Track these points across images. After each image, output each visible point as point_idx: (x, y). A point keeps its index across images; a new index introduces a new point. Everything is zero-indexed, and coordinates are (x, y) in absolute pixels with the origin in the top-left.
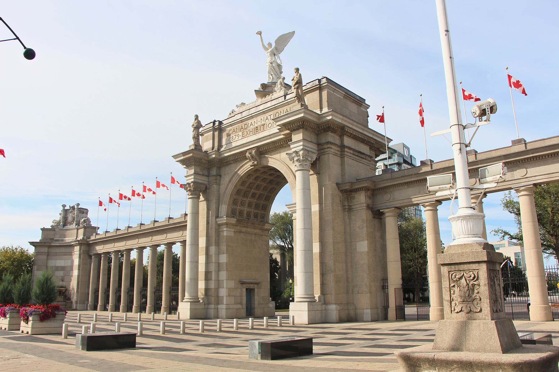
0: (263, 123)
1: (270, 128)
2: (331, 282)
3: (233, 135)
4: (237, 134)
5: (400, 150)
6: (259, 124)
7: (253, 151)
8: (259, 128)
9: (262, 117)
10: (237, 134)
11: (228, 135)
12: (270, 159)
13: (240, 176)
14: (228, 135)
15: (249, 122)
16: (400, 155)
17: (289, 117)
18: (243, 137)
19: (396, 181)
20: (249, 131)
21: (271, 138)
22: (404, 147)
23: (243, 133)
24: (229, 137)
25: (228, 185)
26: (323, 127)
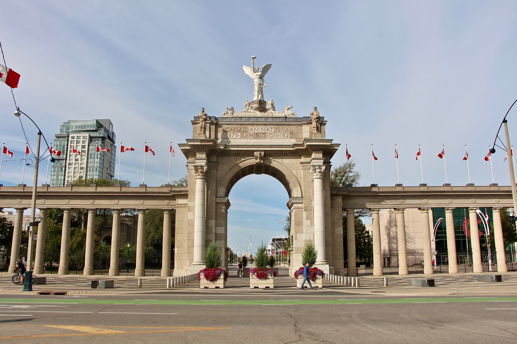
0: (263, 132)
3: (231, 133)
4: (235, 133)
5: (106, 125)
7: (262, 153)
9: (263, 127)
11: (225, 132)
12: (272, 161)
13: (241, 168)
14: (225, 132)
15: (250, 127)
16: (107, 131)
17: (318, 142)
18: (242, 137)
19: (360, 194)
20: (249, 134)
21: (281, 148)
22: (110, 123)
24: (226, 133)
25: (228, 172)
26: (327, 152)
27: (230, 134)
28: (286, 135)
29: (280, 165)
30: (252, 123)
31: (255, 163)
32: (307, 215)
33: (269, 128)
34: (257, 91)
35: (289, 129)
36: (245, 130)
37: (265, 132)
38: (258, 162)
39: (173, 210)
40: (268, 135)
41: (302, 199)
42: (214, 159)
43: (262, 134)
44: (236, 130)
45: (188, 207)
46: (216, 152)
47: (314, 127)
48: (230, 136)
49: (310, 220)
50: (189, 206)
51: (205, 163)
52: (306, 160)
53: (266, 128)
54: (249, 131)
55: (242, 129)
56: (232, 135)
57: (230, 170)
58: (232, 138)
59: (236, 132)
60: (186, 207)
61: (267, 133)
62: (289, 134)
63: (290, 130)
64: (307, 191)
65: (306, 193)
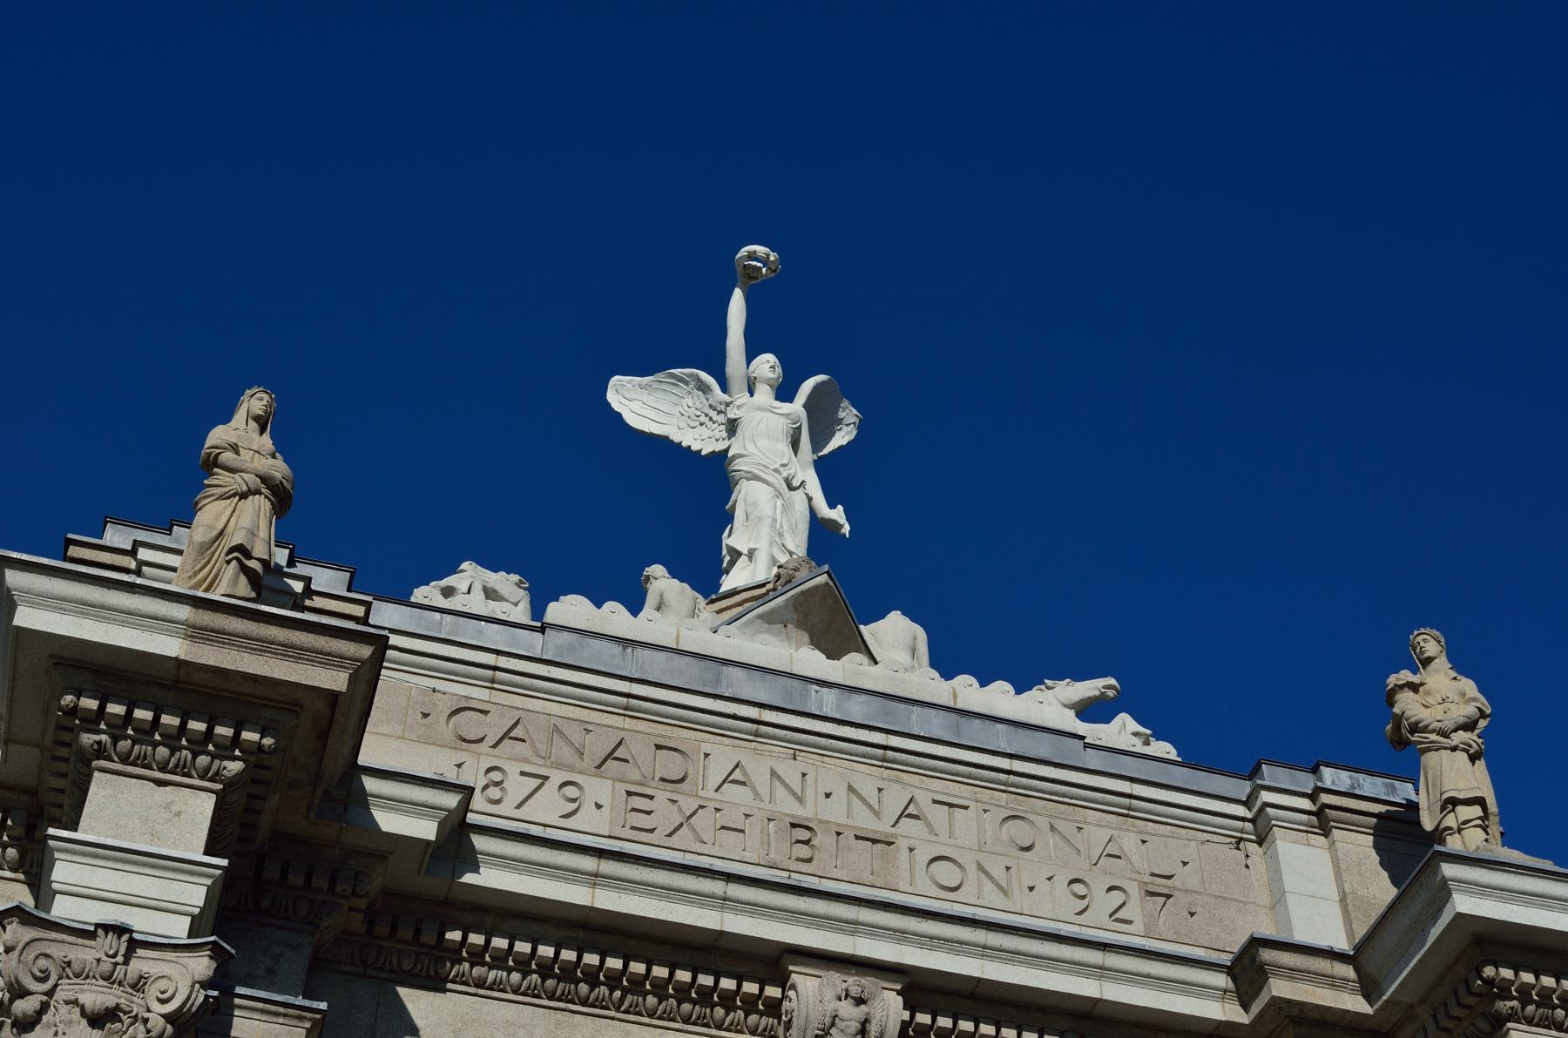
0: (866, 822)
1: (952, 896)
4: (557, 777)
6: (835, 811)
8: (823, 839)
9: (867, 778)
10: (557, 777)
15: (722, 755)
21: (1102, 972)
27: (495, 776)
33: (924, 799)
34: (768, 522)
36: (670, 765)
37: (882, 827)
43: (849, 835)
46: (320, 882)
51: (178, 928)
53: (894, 802)
55: (639, 749)
56: (517, 787)
59: (559, 766)
61: (902, 844)
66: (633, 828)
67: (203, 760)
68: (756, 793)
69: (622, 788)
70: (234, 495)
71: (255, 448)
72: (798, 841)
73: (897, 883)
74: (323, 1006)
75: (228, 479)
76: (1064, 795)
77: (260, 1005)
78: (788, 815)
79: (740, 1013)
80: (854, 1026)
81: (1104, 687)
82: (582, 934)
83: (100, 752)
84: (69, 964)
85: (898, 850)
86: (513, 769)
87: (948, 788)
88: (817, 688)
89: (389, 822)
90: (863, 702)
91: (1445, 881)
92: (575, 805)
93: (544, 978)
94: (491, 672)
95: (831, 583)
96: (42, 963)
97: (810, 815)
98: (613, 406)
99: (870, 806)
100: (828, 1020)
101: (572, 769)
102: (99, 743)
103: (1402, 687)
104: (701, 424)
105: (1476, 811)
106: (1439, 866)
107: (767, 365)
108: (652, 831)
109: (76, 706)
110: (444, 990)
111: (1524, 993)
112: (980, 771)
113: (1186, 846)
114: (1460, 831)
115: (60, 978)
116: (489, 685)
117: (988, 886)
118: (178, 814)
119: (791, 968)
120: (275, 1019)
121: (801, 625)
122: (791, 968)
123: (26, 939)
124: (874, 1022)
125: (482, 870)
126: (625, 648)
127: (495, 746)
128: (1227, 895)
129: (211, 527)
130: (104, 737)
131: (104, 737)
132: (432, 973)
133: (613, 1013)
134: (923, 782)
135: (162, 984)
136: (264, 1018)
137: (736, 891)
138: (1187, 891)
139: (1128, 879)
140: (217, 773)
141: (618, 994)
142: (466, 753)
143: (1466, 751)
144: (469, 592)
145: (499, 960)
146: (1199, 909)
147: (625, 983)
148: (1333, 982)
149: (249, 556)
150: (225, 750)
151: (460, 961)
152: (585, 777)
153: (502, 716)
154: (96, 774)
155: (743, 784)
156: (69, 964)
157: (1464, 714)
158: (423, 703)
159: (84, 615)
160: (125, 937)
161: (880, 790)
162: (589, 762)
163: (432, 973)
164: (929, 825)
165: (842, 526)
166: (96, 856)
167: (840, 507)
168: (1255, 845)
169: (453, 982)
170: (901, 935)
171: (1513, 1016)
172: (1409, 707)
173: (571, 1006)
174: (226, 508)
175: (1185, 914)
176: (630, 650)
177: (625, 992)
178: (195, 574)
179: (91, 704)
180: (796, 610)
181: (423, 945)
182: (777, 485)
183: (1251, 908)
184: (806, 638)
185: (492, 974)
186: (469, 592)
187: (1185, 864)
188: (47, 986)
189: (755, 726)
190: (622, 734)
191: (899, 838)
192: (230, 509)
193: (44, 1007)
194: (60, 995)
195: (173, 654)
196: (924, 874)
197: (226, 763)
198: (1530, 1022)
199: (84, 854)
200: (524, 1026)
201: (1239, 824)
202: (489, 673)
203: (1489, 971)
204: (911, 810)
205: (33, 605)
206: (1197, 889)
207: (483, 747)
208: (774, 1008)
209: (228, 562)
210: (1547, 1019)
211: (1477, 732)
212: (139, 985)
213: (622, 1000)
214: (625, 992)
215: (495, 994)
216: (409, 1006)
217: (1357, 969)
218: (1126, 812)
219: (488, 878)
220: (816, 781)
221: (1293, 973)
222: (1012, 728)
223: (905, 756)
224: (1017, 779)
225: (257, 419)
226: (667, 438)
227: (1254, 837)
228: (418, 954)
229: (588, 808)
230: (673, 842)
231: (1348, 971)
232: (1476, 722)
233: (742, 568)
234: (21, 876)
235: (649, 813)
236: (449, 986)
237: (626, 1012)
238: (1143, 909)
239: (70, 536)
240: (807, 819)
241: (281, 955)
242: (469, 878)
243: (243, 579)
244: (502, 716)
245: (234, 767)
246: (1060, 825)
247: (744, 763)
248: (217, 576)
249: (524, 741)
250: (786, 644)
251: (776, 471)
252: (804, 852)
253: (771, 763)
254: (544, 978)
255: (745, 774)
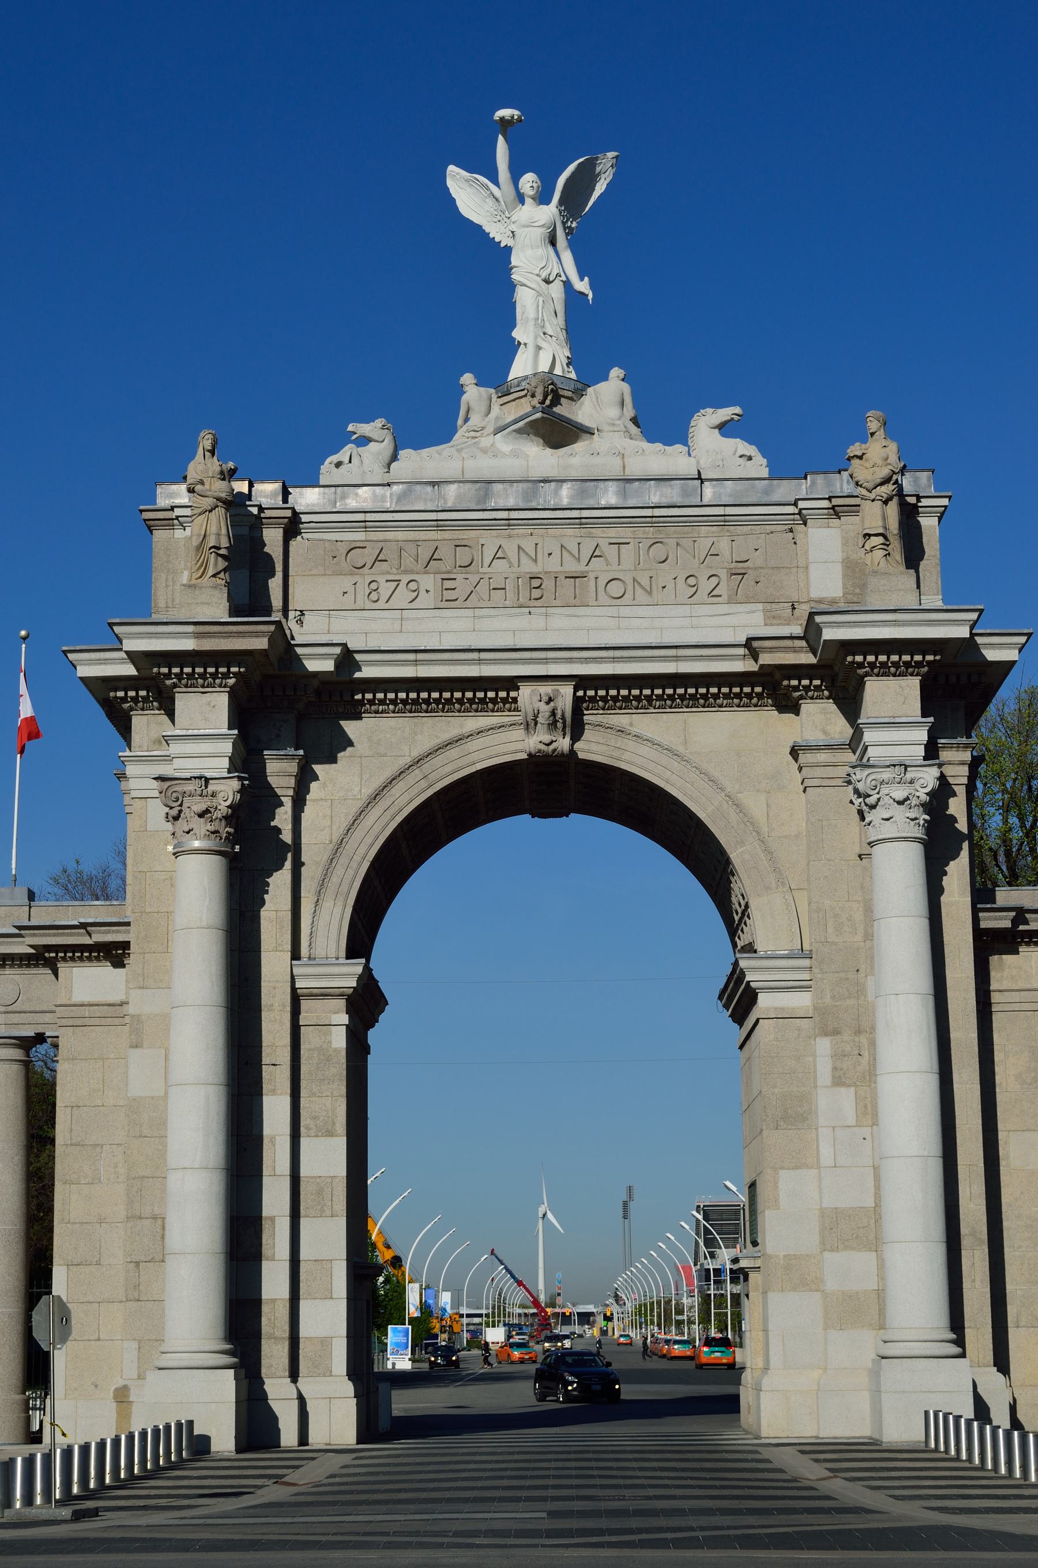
0: (571, 566)
2: (974, 1281)
4: (405, 579)
6: (553, 565)
8: (548, 584)
10: (405, 579)
15: (490, 541)
18: (447, 602)
21: (677, 659)
23: (448, 584)
27: (374, 586)
28: (706, 586)
29: (675, 765)
30: (504, 515)
31: (524, 756)
32: (838, 1056)
33: (604, 544)
34: (532, 323)
35: (724, 545)
37: (581, 568)
38: (543, 747)
39: (40, 1038)
40: (602, 583)
41: (806, 963)
42: (278, 736)
43: (561, 577)
44: (408, 561)
45: (127, 1020)
47: (867, 536)
48: (374, 596)
49: (852, 1089)
50: (137, 1018)
51: (225, 763)
52: (825, 732)
54: (487, 561)
55: (445, 552)
56: (386, 589)
57: (376, 796)
58: (387, 606)
59: (406, 572)
60: (116, 1021)
61: (592, 576)
62: (723, 574)
63: (727, 553)
64: (836, 916)
65: (830, 930)
66: (447, 601)
67: (218, 681)
68: (510, 562)
69: (439, 576)
70: (206, 511)
71: (211, 475)
72: (534, 588)
73: (588, 602)
74: (301, 752)
75: (201, 502)
76: (685, 522)
77: (275, 757)
78: (528, 573)
79: (501, 704)
80: (548, 714)
81: (733, 414)
82: (417, 684)
83: (175, 686)
84: (185, 792)
85: (588, 579)
86: (381, 580)
87: (618, 532)
88: (542, 484)
89: (312, 666)
90: (568, 488)
91: (818, 624)
92: (416, 593)
93: (405, 706)
94: (364, 523)
95: (545, 416)
96: (175, 795)
97: (540, 570)
98: (451, 191)
99: (574, 556)
100: (536, 712)
101: (412, 572)
102: (174, 683)
103: (853, 457)
104: (499, 221)
105: (881, 540)
106: (814, 618)
107: (529, 181)
108: (456, 600)
109: (159, 672)
110: (361, 718)
111: (872, 665)
112: (636, 519)
113: (758, 538)
114: (872, 551)
115: (183, 797)
116: (364, 530)
117: (639, 591)
118: (214, 707)
119: (519, 684)
120: (283, 761)
121: (537, 434)
122: (519, 684)
123: (166, 787)
124: (559, 709)
125: (363, 668)
126: (434, 486)
127: (371, 568)
128: (780, 566)
129: (199, 535)
130: (175, 680)
131: (175, 680)
132: (353, 711)
133: (441, 714)
134: (604, 532)
135: (222, 794)
136: (278, 761)
137: (484, 655)
138: (755, 568)
139: (722, 568)
140: (226, 684)
141: (441, 706)
142: (357, 576)
143: (881, 500)
144: (350, 462)
145: (382, 702)
146: (762, 579)
147: (443, 701)
148: (795, 650)
149: (219, 548)
150: (226, 676)
151: (365, 705)
152: (419, 575)
153: (373, 548)
154: (176, 695)
155: (504, 558)
156: (185, 792)
157: (881, 477)
158: (332, 550)
159: (150, 638)
160: (203, 779)
161: (579, 544)
162: (420, 566)
163: (353, 711)
164: (607, 560)
165: (587, 295)
166: (185, 739)
167: (586, 279)
168: (803, 526)
169: (364, 713)
170: (570, 660)
171: (867, 674)
172: (856, 470)
173: (420, 714)
174: (204, 520)
175: (753, 583)
176: (436, 487)
177: (444, 705)
178: (198, 561)
179: (165, 670)
180: (532, 428)
181: (345, 701)
182: (538, 289)
183: (795, 570)
184: (541, 441)
185: (381, 708)
186: (350, 462)
187: (757, 550)
188: (179, 803)
189: (507, 521)
190: (436, 543)
191: (590, 573)
192: (206, 519)
193: (180, 811)
194: (185, 805)
195: (191, 648)
196: (603, 593)
197: (228, 680)
198: (878, 675)
199: (180, 740)
200: (399, 729)
201: (792, 517)
202: (363, 524)
203: (850, 659)
204: (596, 553)
205: (128, 638)
206: (760, 566)
207: (366, 570)
208: (515, 700)
209: (211, 553)
210: (886, 673)
211: (892, 482)
212: (213, 795)
213: (444, 708)
214: (444, 705)
215: (384, 715)
216: (346, 729)
217: (807, 642)
218: (723, 523)
219: (367, 672)
220: (543, 547)
221: (771, 650)
222: (658, 482)
223: (592, 520)
224: (657, 519)
225: (209, 451)
226: (481, 226)
227: (801, 522)
228: (344, 705)
229: (423, 593)
230: (468, 604)
231: (803, 643)
232: (892, 476)
233: (523, 353)
234: (163, 712)
235: (454, 589)
236: (363, 715)
237: (447, 712)
238: (728, 586)
239: (142, 507)
240: (539, 573)
241: (281, 726)
242: (357, 675)
243: (220, 559)
244: (373, 548)
245: (232, 681)
246: (683, 542)
247: (503, 545)
248: (207, 561)
249: (386, 561)
250: (531, 443)
251: (538, 275)
252: (536, 593)
253: (518, 541)
254: (405, 706)
255: (504, 552)
